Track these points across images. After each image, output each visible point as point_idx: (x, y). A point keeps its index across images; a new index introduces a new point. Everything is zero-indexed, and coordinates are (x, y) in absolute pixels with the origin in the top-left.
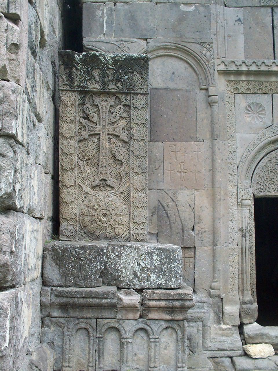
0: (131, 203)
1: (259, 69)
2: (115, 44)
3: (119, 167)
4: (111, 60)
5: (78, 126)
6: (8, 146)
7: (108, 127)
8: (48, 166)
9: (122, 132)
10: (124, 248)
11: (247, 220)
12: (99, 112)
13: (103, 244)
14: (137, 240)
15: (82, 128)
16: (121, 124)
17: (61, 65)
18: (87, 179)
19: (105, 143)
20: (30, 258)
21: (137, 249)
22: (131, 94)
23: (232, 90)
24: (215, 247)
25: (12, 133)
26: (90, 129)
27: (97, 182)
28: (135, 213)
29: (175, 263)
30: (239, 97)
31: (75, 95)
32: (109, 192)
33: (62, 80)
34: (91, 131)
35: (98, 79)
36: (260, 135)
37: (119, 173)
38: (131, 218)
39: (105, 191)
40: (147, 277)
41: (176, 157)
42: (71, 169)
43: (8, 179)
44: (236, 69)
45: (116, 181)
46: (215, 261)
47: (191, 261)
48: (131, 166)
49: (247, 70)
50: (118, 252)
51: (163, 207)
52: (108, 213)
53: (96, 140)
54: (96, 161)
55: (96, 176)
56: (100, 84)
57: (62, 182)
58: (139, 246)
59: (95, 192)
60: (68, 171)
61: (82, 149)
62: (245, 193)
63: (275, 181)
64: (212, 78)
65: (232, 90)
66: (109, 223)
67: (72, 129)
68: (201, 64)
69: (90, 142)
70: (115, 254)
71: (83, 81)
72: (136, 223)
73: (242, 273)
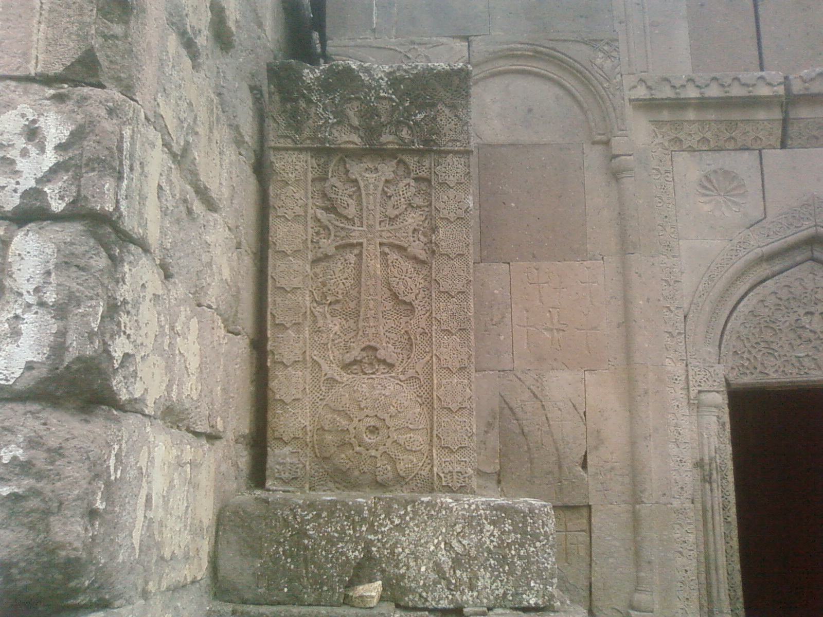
0: (435, 401)
1: (727, 94)
2: (399, 50)
4: (386, 79)
5: (312, 228)
6: (92, 242)
8: (239, 315)
9: (412, 239)
10: (414, 506)
11: (714, 441)
12: (360, 195)
13: (364, 499)
14: (449, 490)
15: (322, 231)
16: (410, 221)
17: (274, 94)
19: (375, 265)
20: (167, 534)
21: (445, 509)
22: (433, 154)
23: (666, 144)
24: (638, 506)
25: (102, 208)
26: (338, 234)
27: (355, 353)
29: (538, 544)
30: (682, 159)
31: (305, 159)
32: (383, 376)
33: (275, 125)
34: (342, 239)
35: (356, 122)
36: (735, 241)
37: (406, 331)
38: (435, 436)
40: (470, 579)
41: (541, 296)
42: (295, 324)
43: (88, 323)
44: (673, 96)
45: (399, 350)
46: (639, 539)
47: (581, 539)
48: (434, 315)
49: (698, 96)
50: (400, 517)
51: (511, 409)
52: (379, 424)
53: (352, 258)
54: (352, 305)
55: (352, 340)
56: (361, 133)
57: (273, 354)
58: (451, 501)
59: (351, 376)
60: (287, 329)
61: (320, 280)
62: (707, 377)
63: (776, 348)
64: (617, 118)
65: (666, 144)
66: (381, 448)
67: (297, 234)
68: (593, 87)
69: (339, 264)
70: (392, 522)
71: (323, 129)
72: (447, 448)
73: (708, 571)
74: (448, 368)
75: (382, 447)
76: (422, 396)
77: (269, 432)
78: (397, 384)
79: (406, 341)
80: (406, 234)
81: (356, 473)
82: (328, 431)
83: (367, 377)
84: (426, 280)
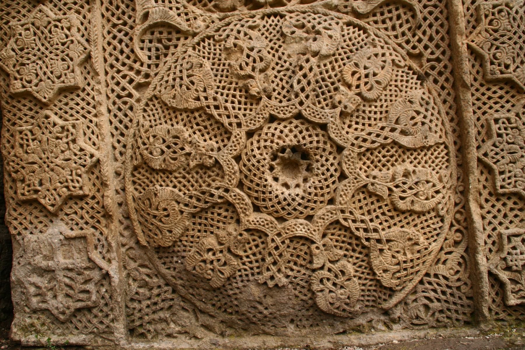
0: (467, 66)
28: (495, 127)
38: (474, 164)
59: (215, 16)
72: (509, 195)
76: (420, 56)
77: (7, 186)
78: (349, 24)
81: (255, 291)
82: (164, 171)
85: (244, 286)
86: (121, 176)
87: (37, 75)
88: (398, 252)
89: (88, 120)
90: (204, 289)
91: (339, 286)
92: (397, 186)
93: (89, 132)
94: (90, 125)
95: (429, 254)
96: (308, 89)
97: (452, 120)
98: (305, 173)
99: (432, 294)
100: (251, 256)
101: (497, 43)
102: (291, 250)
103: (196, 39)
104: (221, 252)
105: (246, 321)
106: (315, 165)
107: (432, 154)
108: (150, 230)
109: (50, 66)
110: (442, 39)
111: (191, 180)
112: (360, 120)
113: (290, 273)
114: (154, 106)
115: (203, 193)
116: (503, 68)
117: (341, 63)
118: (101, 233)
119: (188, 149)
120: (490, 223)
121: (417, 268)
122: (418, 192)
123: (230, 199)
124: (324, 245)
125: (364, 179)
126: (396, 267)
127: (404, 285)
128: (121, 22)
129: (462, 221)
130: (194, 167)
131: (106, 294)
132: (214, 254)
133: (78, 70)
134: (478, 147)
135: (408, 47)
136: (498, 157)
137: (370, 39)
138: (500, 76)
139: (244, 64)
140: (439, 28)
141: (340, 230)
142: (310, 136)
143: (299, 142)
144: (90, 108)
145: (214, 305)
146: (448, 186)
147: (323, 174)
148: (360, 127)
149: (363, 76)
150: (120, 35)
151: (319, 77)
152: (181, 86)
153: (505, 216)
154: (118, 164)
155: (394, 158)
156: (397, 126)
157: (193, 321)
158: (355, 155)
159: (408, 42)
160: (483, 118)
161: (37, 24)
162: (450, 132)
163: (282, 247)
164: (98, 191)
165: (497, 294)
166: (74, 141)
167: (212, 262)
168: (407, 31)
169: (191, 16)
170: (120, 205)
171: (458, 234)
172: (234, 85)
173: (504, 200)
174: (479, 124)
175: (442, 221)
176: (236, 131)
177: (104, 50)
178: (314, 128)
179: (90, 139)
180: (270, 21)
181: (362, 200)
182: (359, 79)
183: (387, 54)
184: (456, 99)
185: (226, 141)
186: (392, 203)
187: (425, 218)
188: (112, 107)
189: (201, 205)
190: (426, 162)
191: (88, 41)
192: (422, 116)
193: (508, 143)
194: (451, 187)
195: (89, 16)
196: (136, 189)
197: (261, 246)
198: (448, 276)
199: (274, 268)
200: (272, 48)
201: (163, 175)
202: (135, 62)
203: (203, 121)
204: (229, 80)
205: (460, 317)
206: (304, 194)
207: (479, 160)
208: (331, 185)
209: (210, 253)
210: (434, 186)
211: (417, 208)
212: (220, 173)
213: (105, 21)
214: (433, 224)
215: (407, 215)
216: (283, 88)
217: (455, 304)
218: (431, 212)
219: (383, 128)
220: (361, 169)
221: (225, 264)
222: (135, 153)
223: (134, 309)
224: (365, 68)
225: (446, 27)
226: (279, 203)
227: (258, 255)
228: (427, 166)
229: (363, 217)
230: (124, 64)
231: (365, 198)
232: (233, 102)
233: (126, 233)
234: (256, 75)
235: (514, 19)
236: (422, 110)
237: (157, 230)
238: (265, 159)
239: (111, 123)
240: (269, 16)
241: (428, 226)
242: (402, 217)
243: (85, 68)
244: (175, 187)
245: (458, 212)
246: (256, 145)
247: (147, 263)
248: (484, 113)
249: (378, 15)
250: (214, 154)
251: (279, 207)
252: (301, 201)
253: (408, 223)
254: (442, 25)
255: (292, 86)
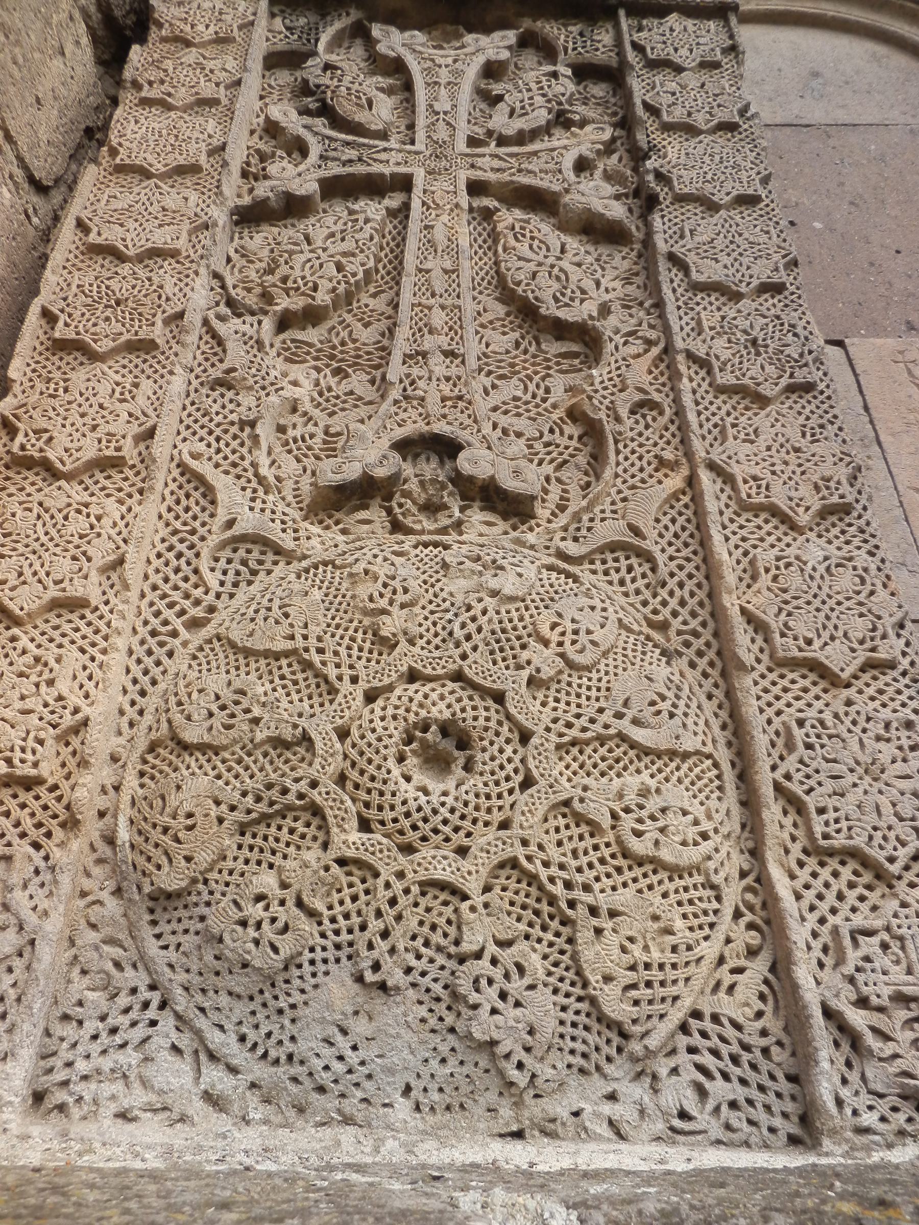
3: (575, 379)
7: (468, 151)
18: (278, 449)
22: (622, 13)
26: (332, 154)
28: (799, 734)
39: (444, 531)
45: (548, 469)
48: (679, 344)
54: (367, 336)
74: (774, 511)
75: (492, 833)
78: (550, 568)
79: (574, 443)
80: (551, 166)
82: (203, 748)
83: (413, 539)
84: (627, 281)
85: (316, 986)
86: (120, 763)
87: (20, 574)
88: (631, 940)
89: (87, 656)
90: (230, 994)
91: (511, 1000)
92: (627, 810)
93: (82, 676)
94: (89, 664)
95: (699, 960)
96: (477, 638)
97: (724, 727)
98: (459, 772)
99: (708, 1060)
100: (340, 918)
101: (789, 607)
102: (421, 910)
103: (305, 564)
104: (282, 903)
105: (308, 1083)
106: (479, 757)
107: (691, 770)
108: (149, 859)
109: (47, 564)
110: (701, 604)
111: (252, 765)
112: (563, 696)
113: (413, 963)
114: (212, 650)
115: (269, 786)
116: (801, 642)
117: (535, 612)
118: (46, 858)
119: (257, 711)
120: (812, 908)
121: (673, 990)
122: (666, 826)
123: (318, 800)
124: (486, 905)
125: (566, 790)
126: (629, 973)
127: (649, 1025)
128: (188, 528)
129: (758, 907)
130: (263, 743)
131: (11, 991)
132: (266, 908)
133: (94, 577)
134: (774, 768)
135: (647, 610)
136: (812, 782)
137: (583, 589)
138: (797, 654)
139: (376, 594)
140: (695, 589)
141: (519, 882)
142: (474, 708)
143: (454, 715)
144: (98, 638)
145: (242, 1039)
146: (724, 830)
147: (493, 773)
148: (562, 706)
149: (569, 631)
150: (181, 547)
151: (497, 627)
152: (265, 619)
153: (840, 897)
154: (122, 740)
155: (621, 764)
156: (624, 710)
157: (187, 1079)
158: (552, 747)
159: (645, 603)
160: (777, 721)
161: (46, 505)
162: (722, 741)
163: (402, 901)
164: (68, 777)
165: (849, 1064)
166: (51, 683)
167: (259, 925)
168: (643, 589)
169: (301, 533)
170: (102, 814)
171: (753, 933)
172: (355, 623)
173: (834, 863)
174: (771, 730)
175: (718, 899)
176: (345, 686)
177: (149, 562)
178: (483, 699)
179: (81, 686)
180: (426, 551)
181: (562, 828)
182: (563, 634)
183: (611, 610)
184: (729, 694)
185: (327, 704)
186: (619, 841)
187: (683, 883)
188: (136, 647)
189: (262, 807)
190: (680, 781)
191: (125, 541)
192: (668, 703)
193: (828, 761)
194: (729, 835)
195: (136, 509)
196: (142, 786)
197: (363, 898)
198: (741, 1020)
199: (383, 946)
200: (425, 582)
201: (200, 757)
202: (196, 586)
203: (293, 673)
204: (347, 617)
205: (778, 1122)
206: (455, 804)
207: (778, 787)
208: (505, 794)
209: (261, 905)
210: (696, 823)
211: (665, 855)
212: (308, 756)
213: (161, 524)
214: (700, 899)
215: (648, 868)
216: (436, 635)
217: (762, 1088)
218: (695, 872)
219: (601, 711)
220: (561, 774)
221: (286, 929)
222: (158, 721)
223: (62, 1039)
224: (573, 621)
225: (706, 587)
226: (408, 815)
227: (354, 915)
228: (682, 787)
229: (563, 859)
230: (176, 588)
231: (567, 827)
232: (349, 648)
233: (96, 871)
234: (395, 610)
235: (811, 577)
236: (670, 694)
237: (164, 858)
238: (390, 736)
239: (128, 671)
240: (426, 545)
241: (691, 902)
242: (638, 872)
243: (109, 578)
244: (219, 777)
245: (748, 889)
246: (378, 712)
247: (121, 936)
248: (779, 713)
249: (598, 563)
250: (303, 722)
251: (406, 823)
252: (448, 815)
253: (650, 887)
254: (699, 586)
255: (451, 634)
